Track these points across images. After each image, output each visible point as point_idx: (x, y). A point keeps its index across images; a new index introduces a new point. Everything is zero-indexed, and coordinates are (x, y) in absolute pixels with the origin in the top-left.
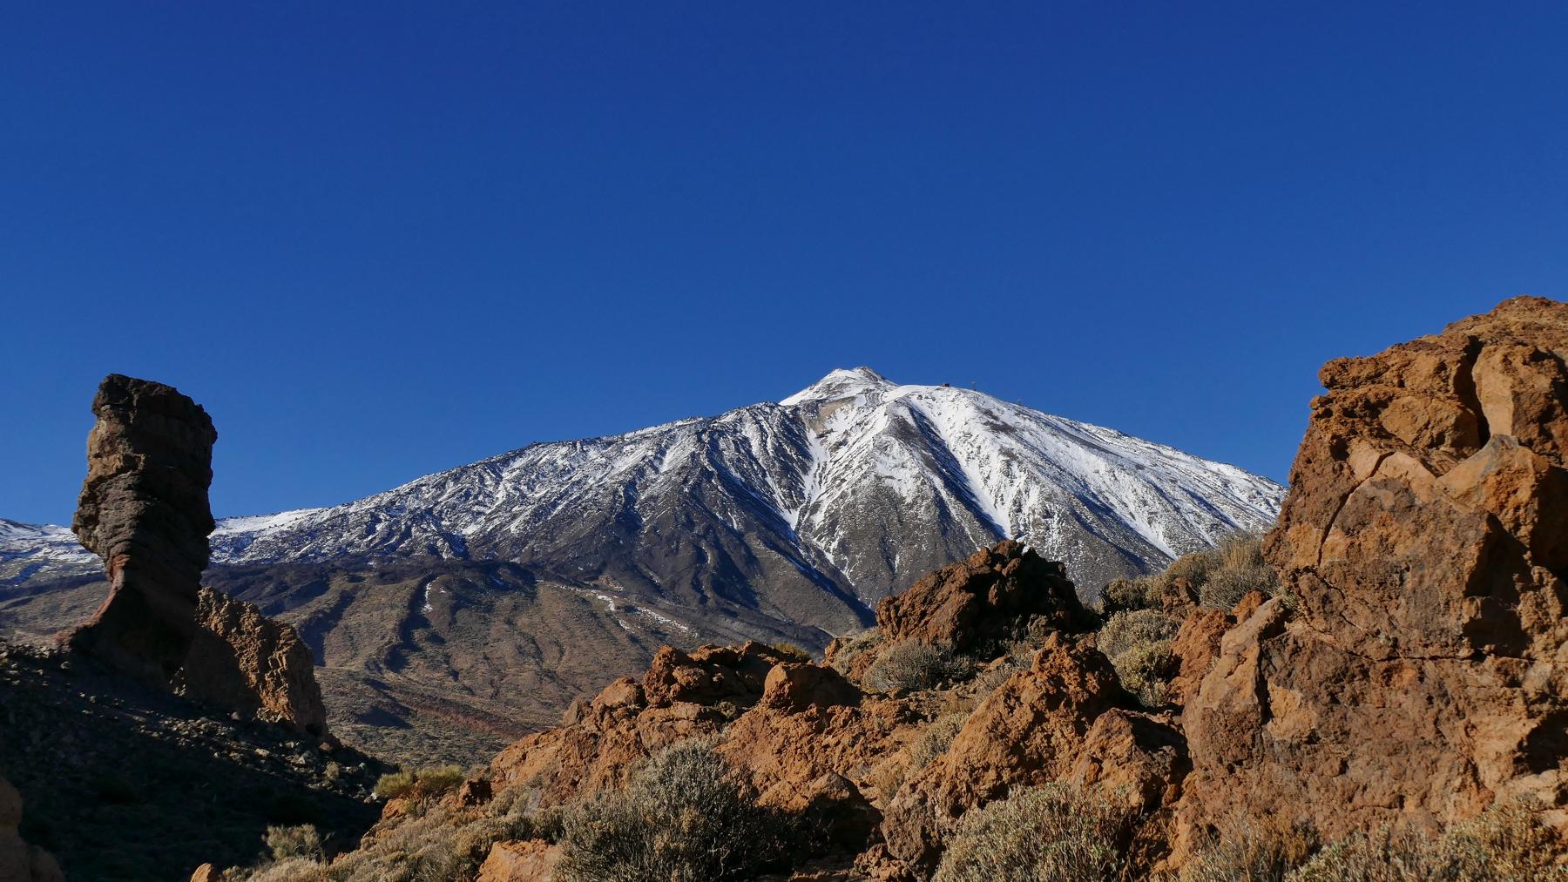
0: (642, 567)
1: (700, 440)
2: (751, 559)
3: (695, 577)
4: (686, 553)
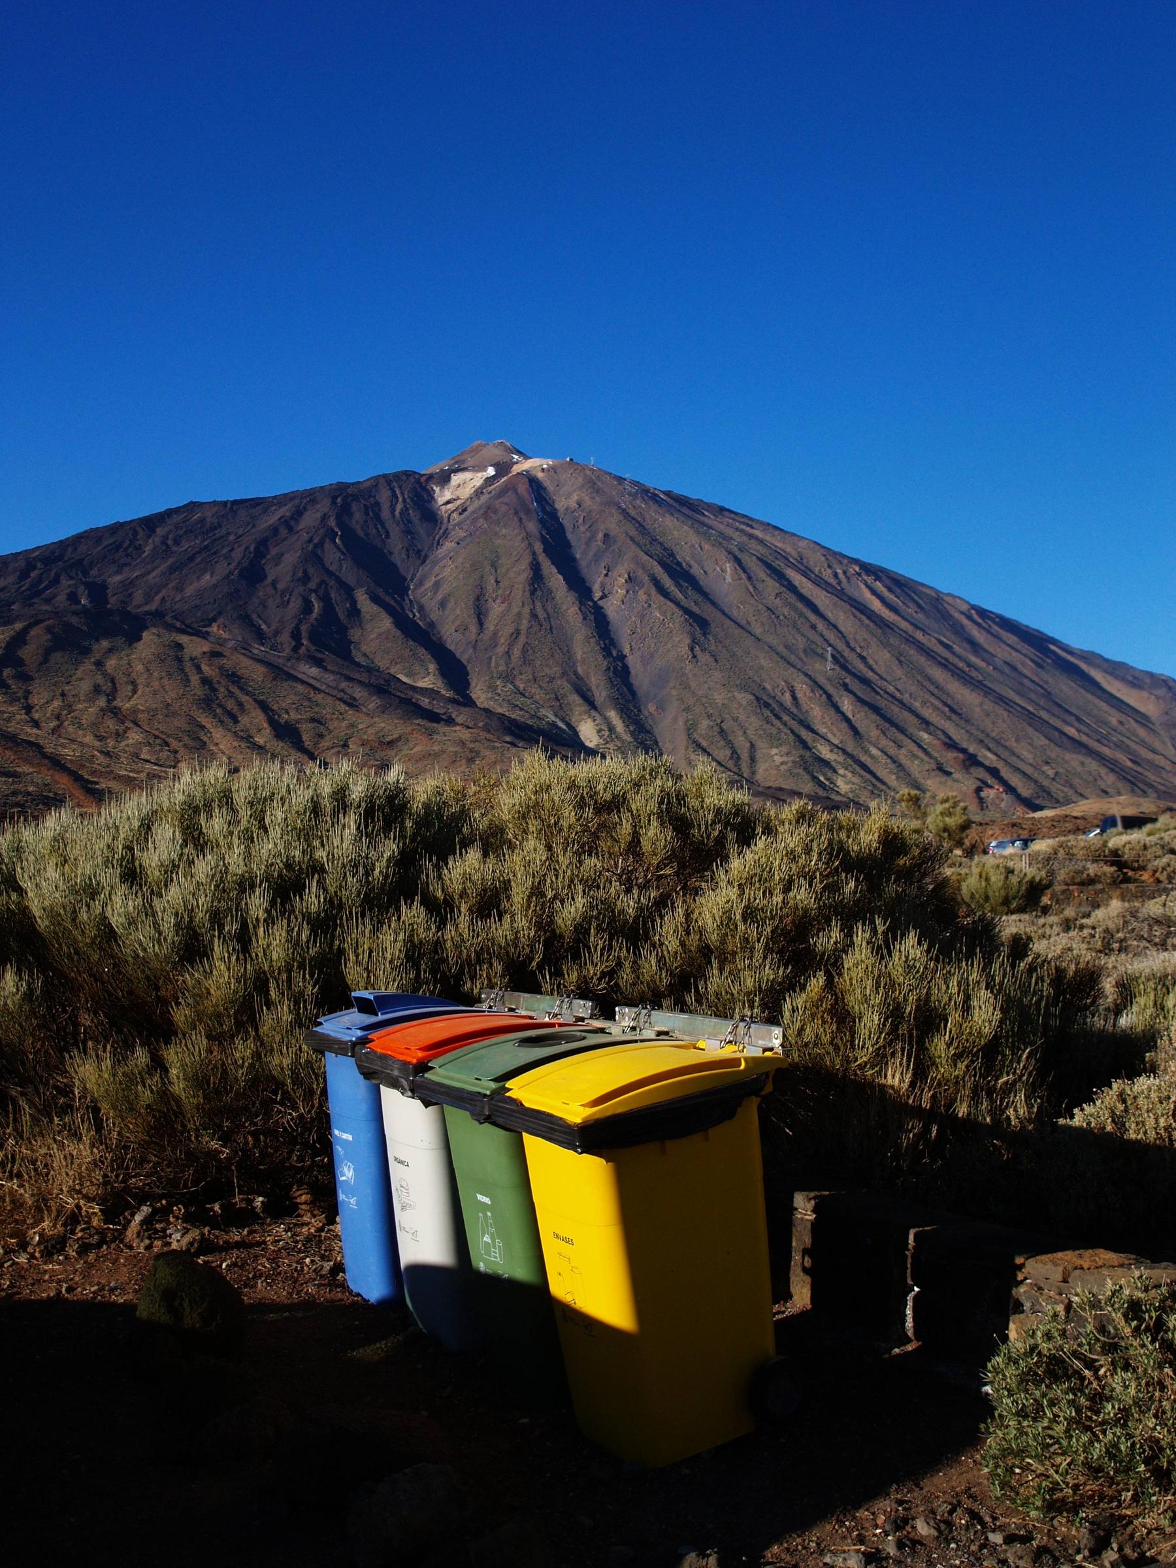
0: (254, 616)
1: (334, 502)
2: (355, 612)
3: (297, 628)
4: (295, 604)
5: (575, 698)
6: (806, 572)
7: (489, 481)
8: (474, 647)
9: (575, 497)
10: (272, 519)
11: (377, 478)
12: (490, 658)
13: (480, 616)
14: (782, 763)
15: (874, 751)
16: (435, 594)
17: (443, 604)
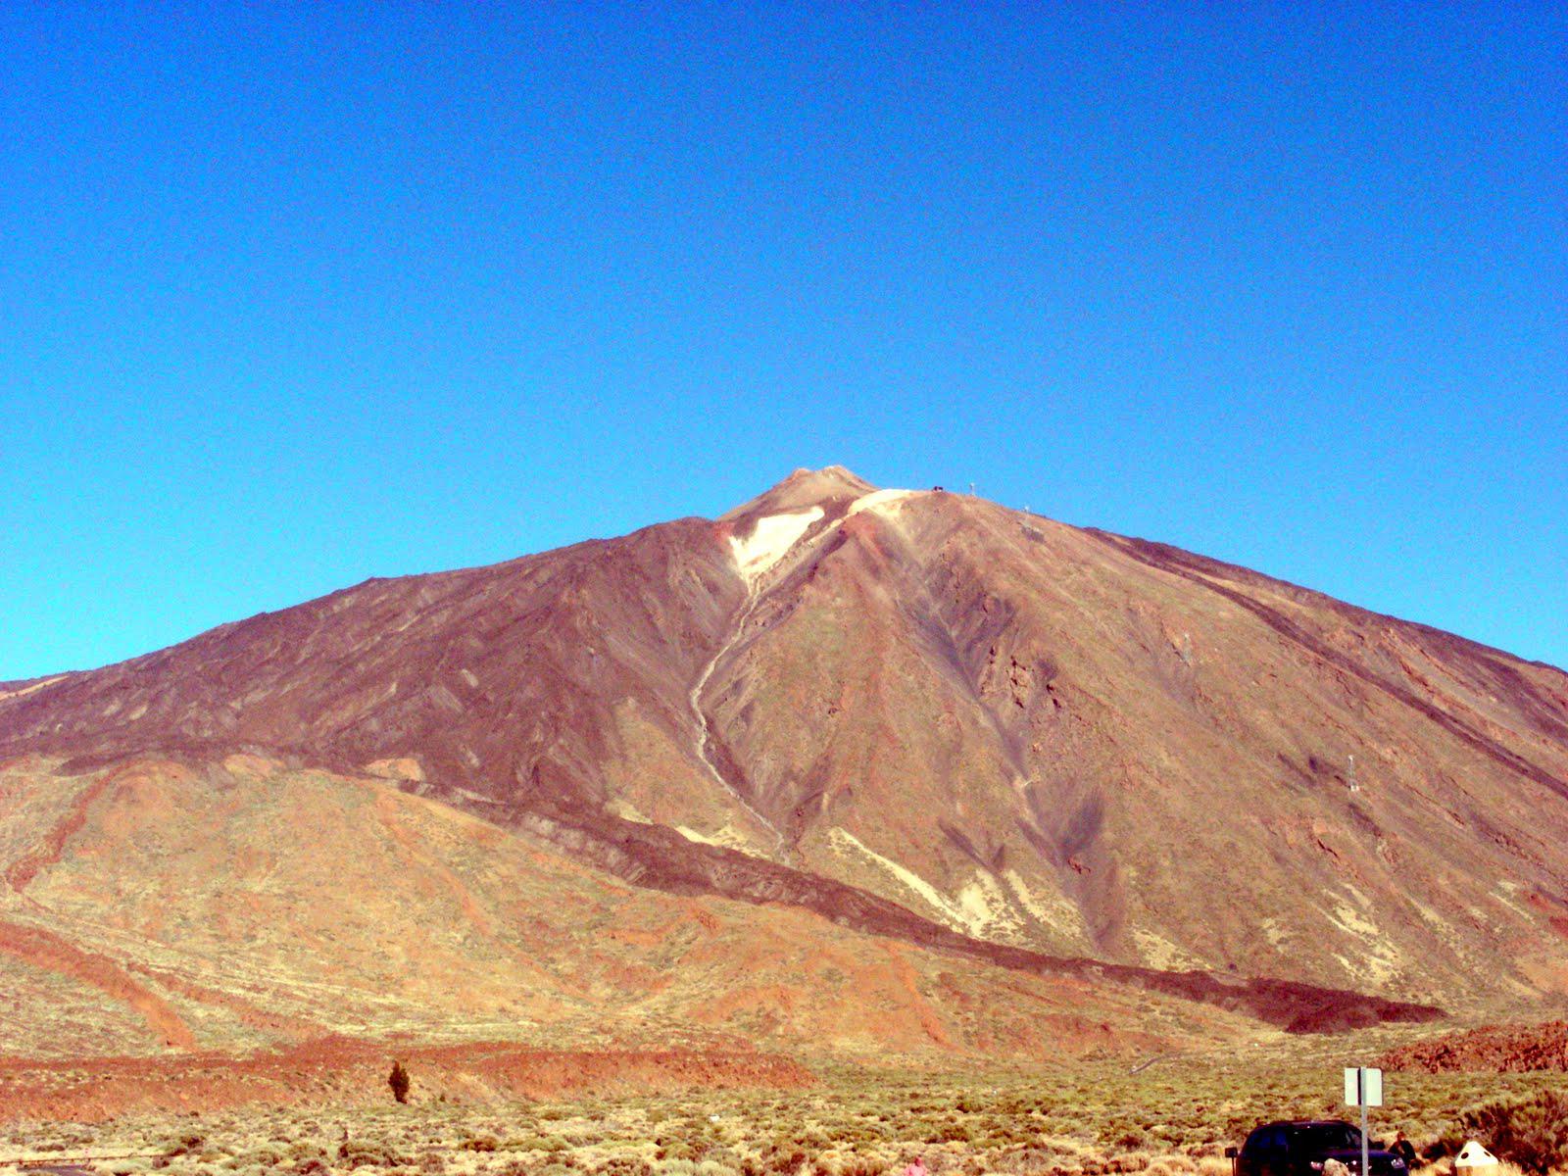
5: (950, 853)
6: (1310, 643)
7: (814, 529)
8: (795, 779)
9: (945, 548)
11: (643, 533)
12: (819, 795)
14: (1281, 941)
15: (1429, 914)
16: (736, 701)
17: (746, 714)
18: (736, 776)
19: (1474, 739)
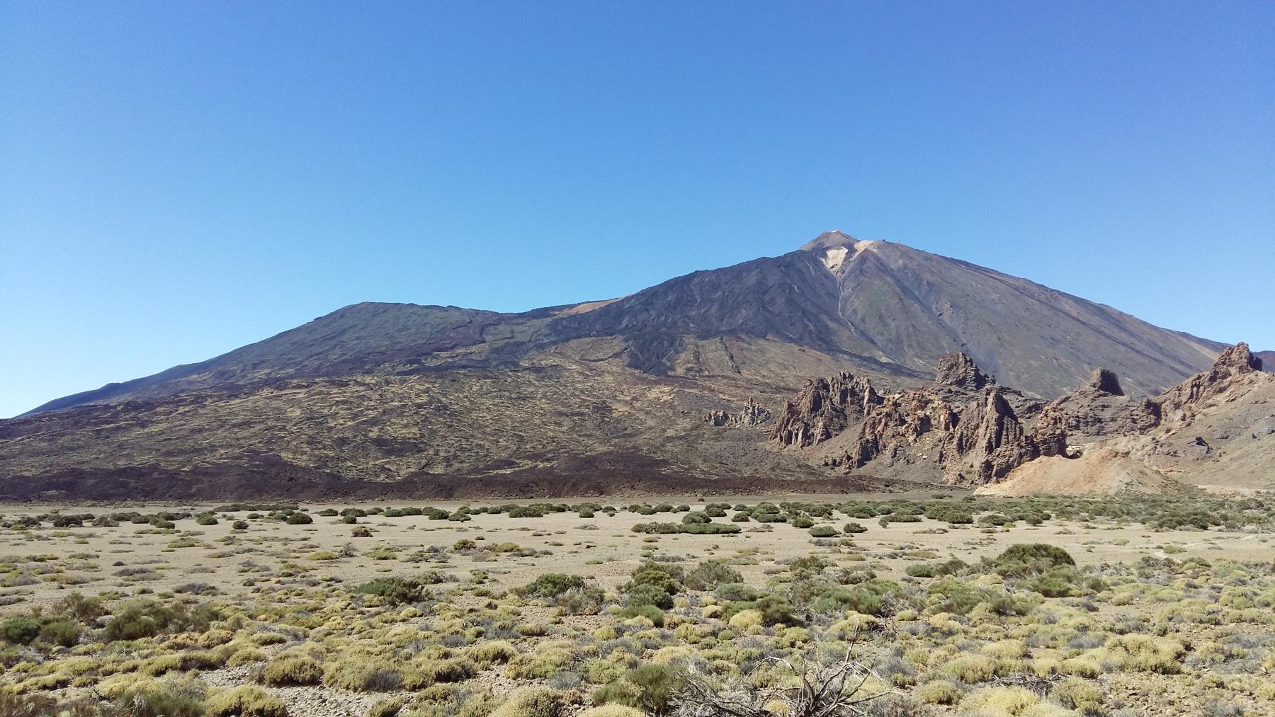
2: (827, 327)
6: (1032, 296)
7: (849, 255)
9: (901, 262)
10: (752, 279)
13: (885, 325)
17: (863, 320)
18: (874, 343)
19: (1098, 331)
